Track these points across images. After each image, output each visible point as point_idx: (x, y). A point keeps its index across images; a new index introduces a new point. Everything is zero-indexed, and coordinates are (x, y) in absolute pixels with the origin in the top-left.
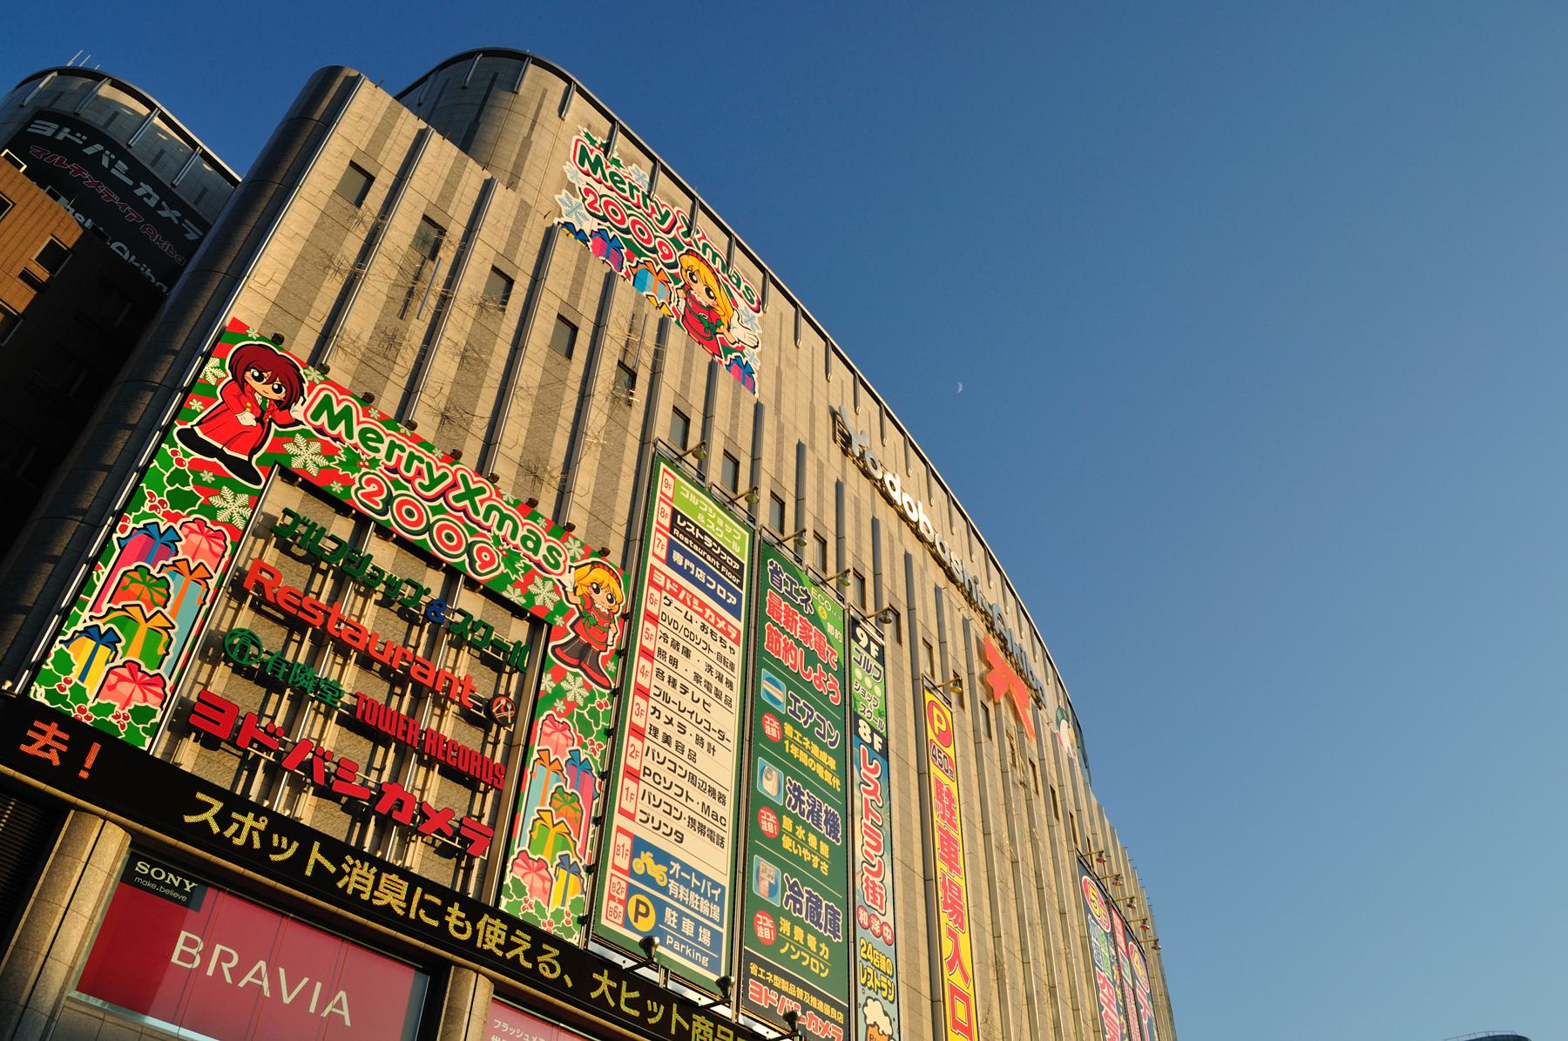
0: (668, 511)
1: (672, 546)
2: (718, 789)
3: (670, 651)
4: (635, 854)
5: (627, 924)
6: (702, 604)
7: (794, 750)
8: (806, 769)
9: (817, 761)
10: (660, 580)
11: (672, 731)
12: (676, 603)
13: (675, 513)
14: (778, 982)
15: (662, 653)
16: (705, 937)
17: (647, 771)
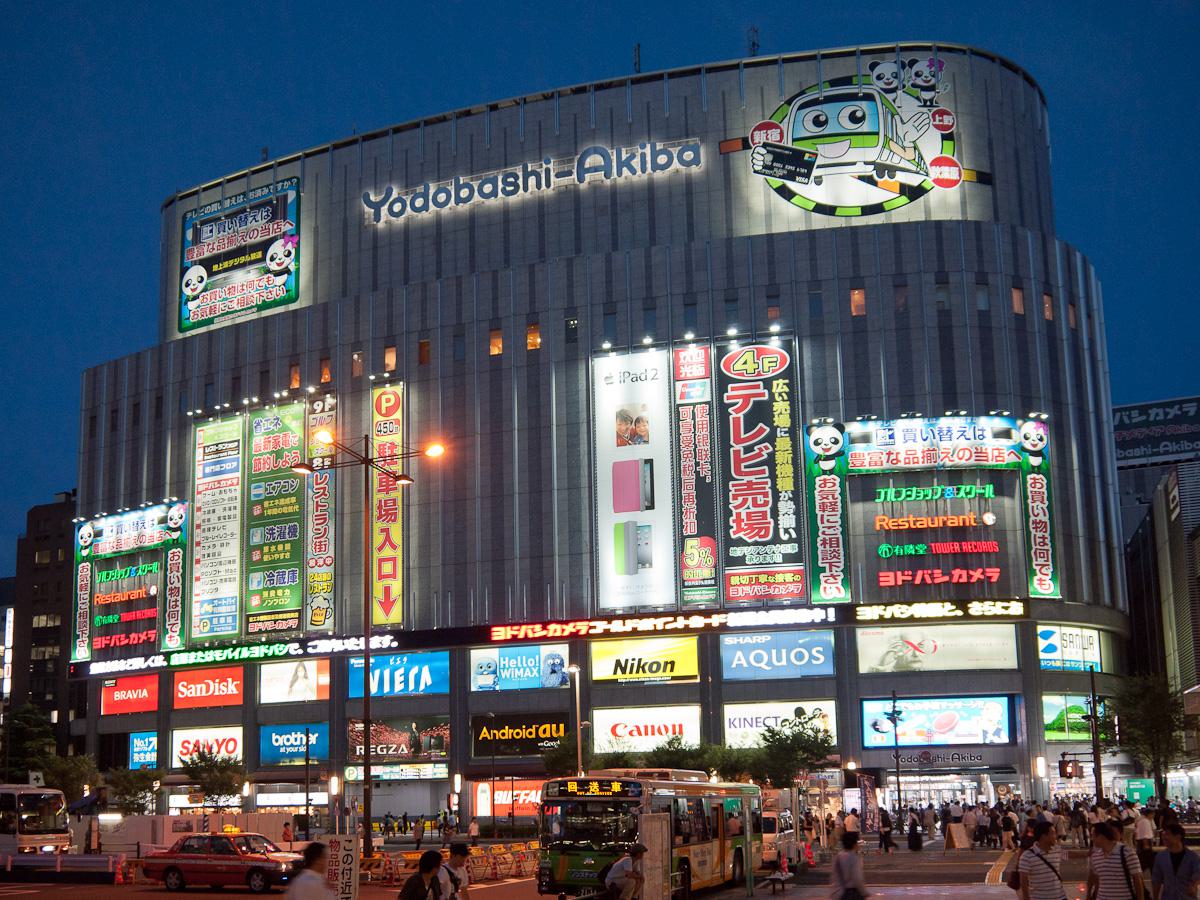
0: (201, 450)
1: (205, 466)
2: (231, 559)
3: (207, 517)
4: (202, 607)
5: (201, 632)
6: (219, 482)
7: (269, 512)
8: (279, 515)
9: (287, 505)
10: (201, 488)
11: (211, 551)
12: (209, 492)
13: (204, 448)
14: (262, 618)
15: (204, 521)
16: (230, 620)
17: (203, 574)
